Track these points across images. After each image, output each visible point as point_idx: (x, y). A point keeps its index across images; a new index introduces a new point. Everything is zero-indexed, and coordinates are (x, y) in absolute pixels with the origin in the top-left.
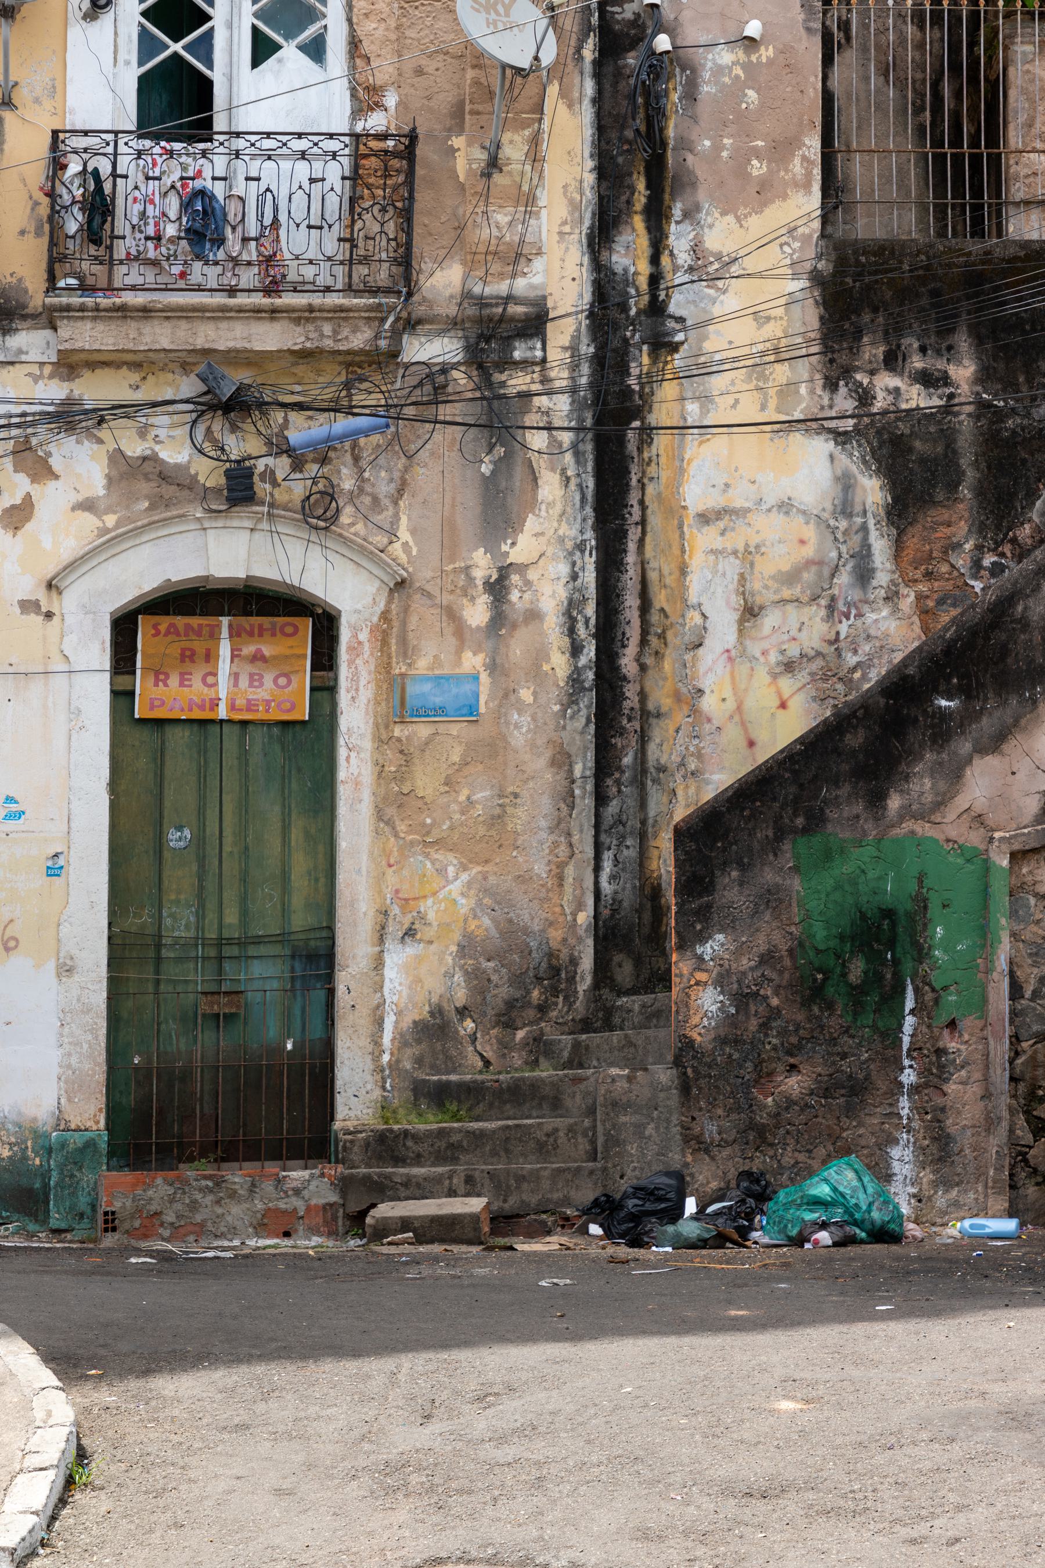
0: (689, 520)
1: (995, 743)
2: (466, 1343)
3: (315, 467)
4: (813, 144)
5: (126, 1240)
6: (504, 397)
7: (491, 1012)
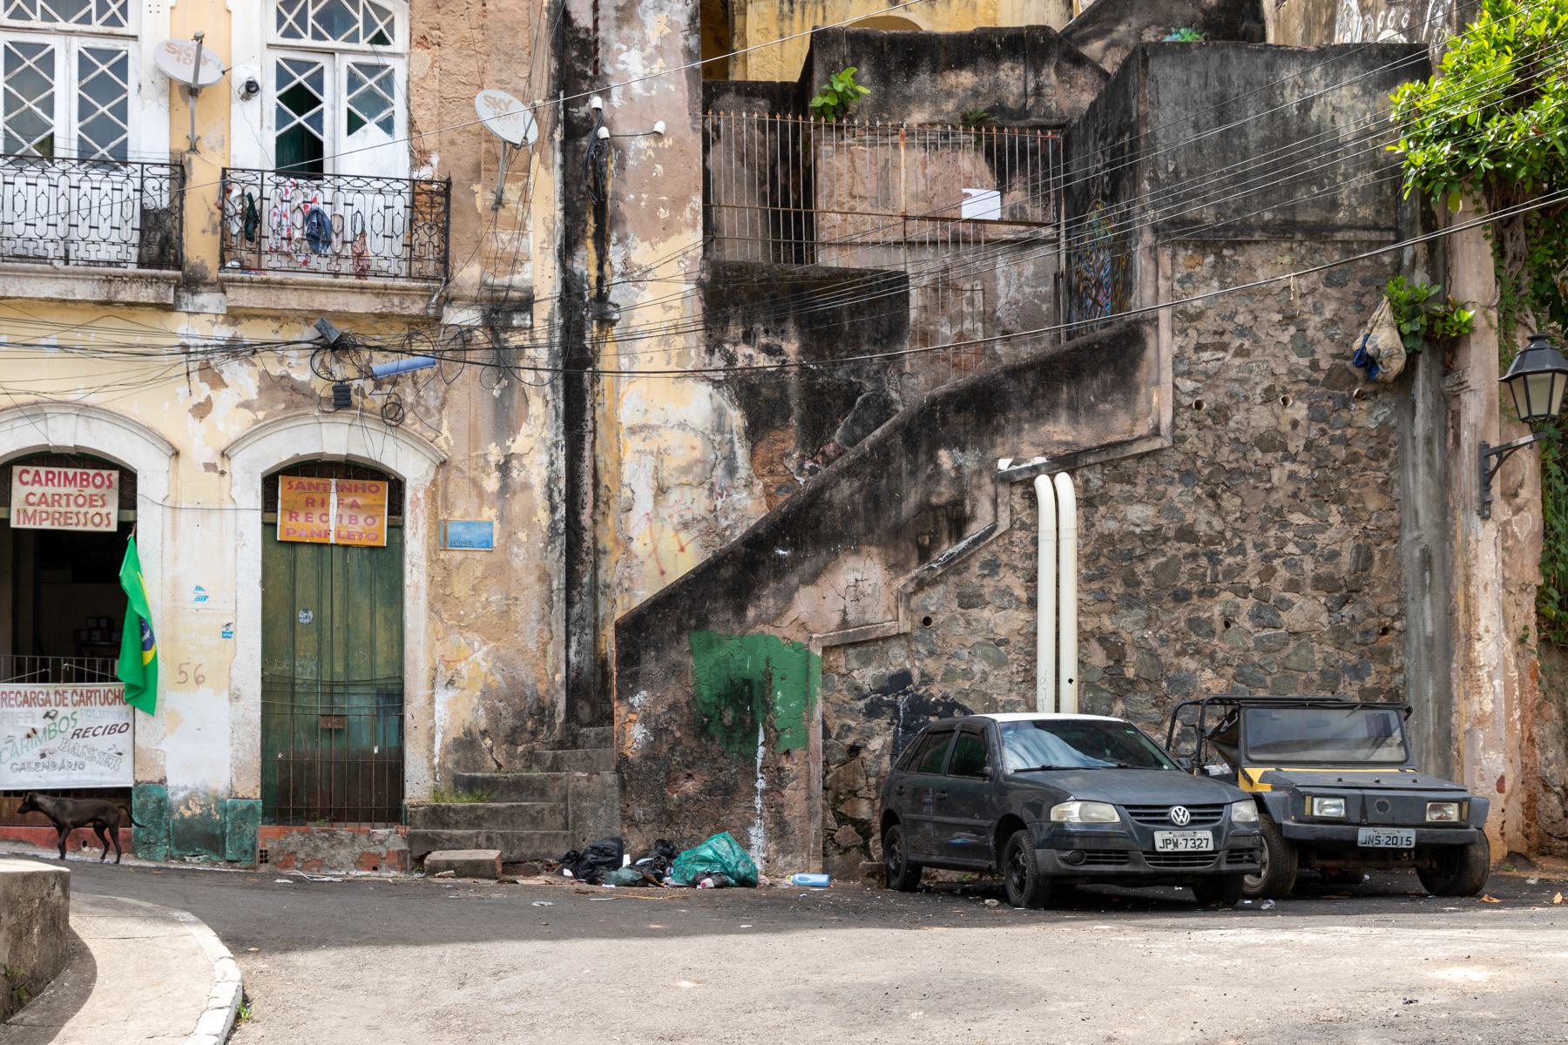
0: (623, 431)
1: (813, 579)
2: (487, 939)
3: (389, 387)
4: (697, 201)
5: (273, 868)
6: (506, 348)
7: (502, 734)
